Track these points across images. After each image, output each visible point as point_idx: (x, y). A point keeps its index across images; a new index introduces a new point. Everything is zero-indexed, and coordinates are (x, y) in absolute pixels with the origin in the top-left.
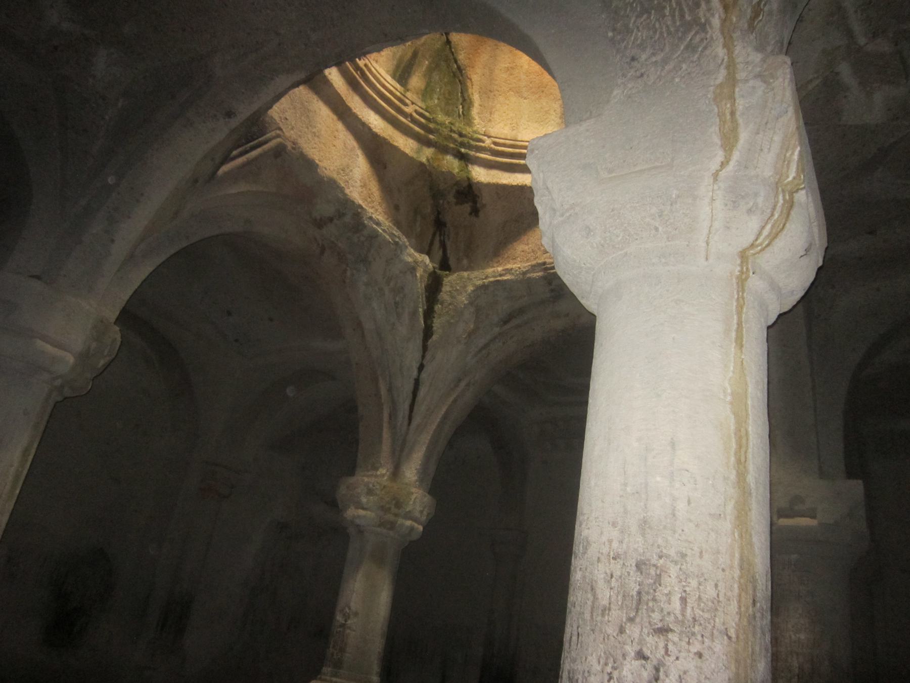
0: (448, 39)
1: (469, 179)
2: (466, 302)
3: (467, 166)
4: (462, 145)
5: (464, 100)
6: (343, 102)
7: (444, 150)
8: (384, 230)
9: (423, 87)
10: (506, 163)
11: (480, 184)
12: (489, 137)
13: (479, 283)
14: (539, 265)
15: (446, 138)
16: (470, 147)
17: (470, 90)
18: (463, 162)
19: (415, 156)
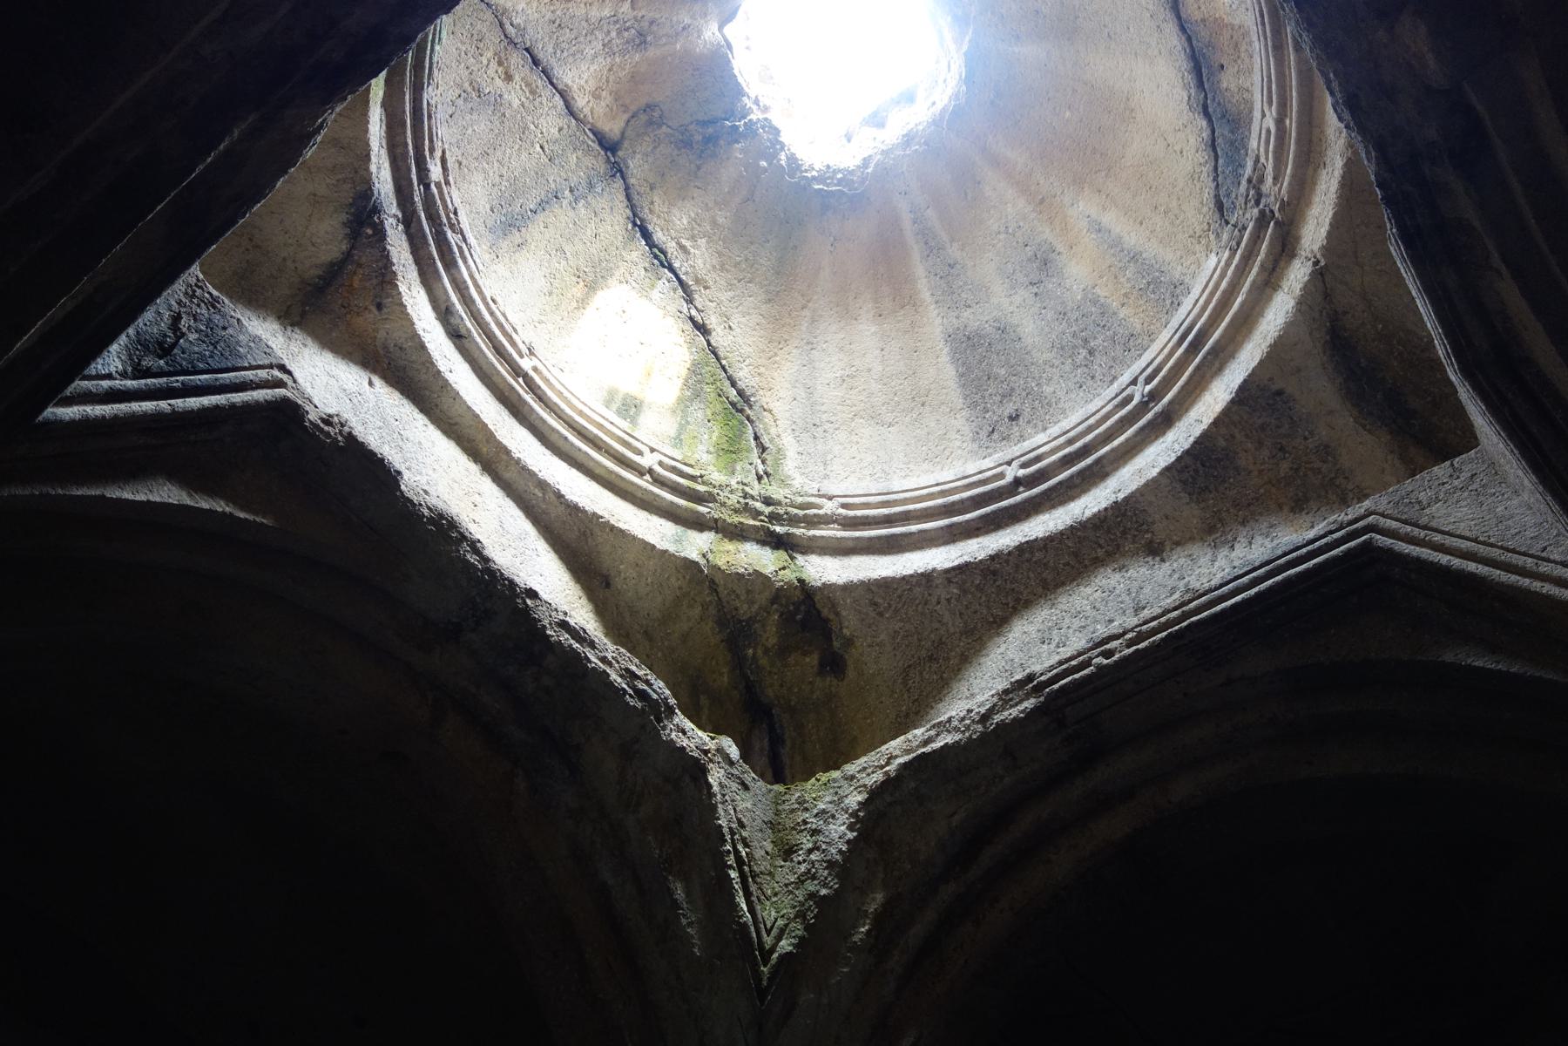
0: (709, 344)
1: (801, 581)
2: (851, 835)
3: (792, 558)
4: (774, 517)
5: (764, 449)
6: (490, 436)
7: (736, 533)
8: (604, 660)
9: (673, 433)
10: (879, 538)
11: (828, 588)
12: (830, 498)
13: (878, 777)
14: (1020, 684)
15: (736, 511)
16: (793, 521)
17: (773, 431)
18: (782, 555)
19: (672, 549)
